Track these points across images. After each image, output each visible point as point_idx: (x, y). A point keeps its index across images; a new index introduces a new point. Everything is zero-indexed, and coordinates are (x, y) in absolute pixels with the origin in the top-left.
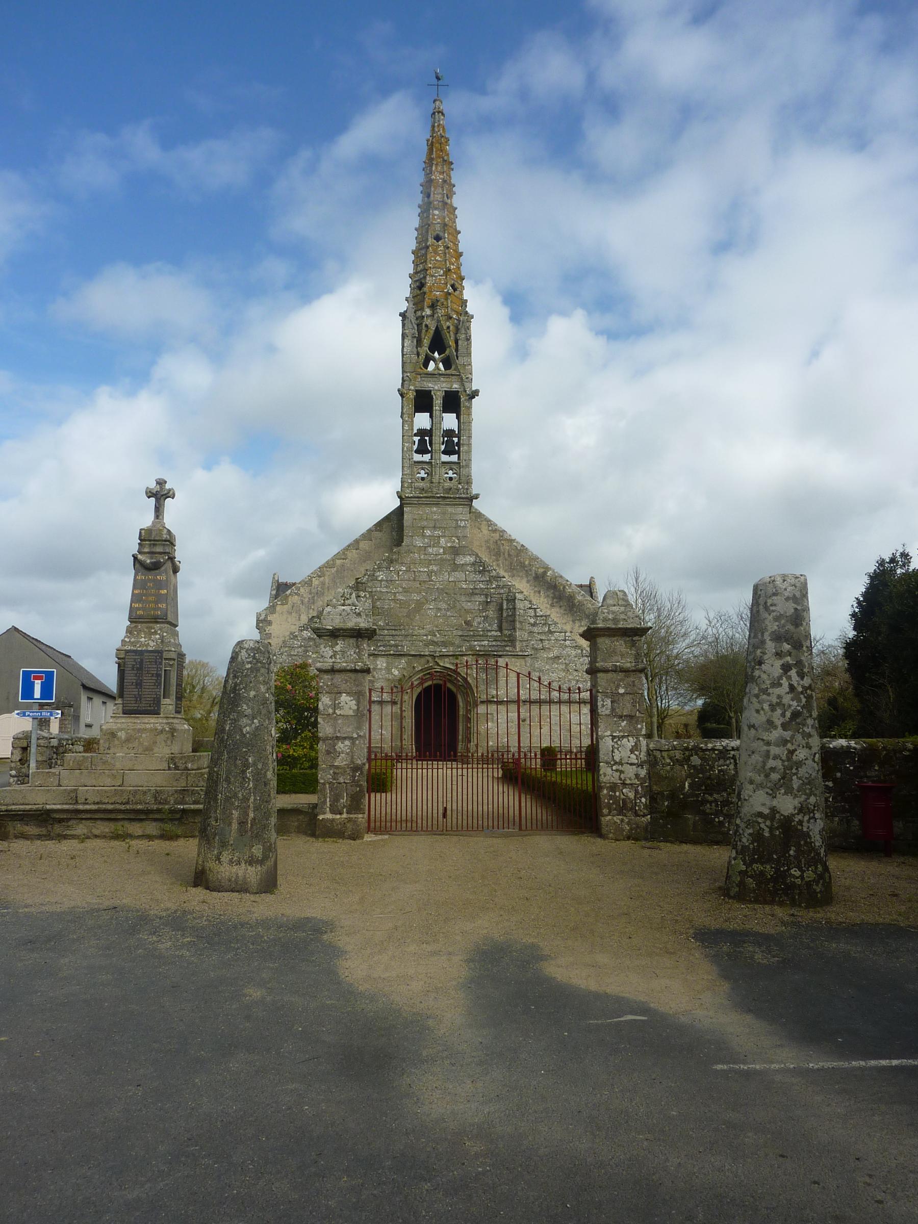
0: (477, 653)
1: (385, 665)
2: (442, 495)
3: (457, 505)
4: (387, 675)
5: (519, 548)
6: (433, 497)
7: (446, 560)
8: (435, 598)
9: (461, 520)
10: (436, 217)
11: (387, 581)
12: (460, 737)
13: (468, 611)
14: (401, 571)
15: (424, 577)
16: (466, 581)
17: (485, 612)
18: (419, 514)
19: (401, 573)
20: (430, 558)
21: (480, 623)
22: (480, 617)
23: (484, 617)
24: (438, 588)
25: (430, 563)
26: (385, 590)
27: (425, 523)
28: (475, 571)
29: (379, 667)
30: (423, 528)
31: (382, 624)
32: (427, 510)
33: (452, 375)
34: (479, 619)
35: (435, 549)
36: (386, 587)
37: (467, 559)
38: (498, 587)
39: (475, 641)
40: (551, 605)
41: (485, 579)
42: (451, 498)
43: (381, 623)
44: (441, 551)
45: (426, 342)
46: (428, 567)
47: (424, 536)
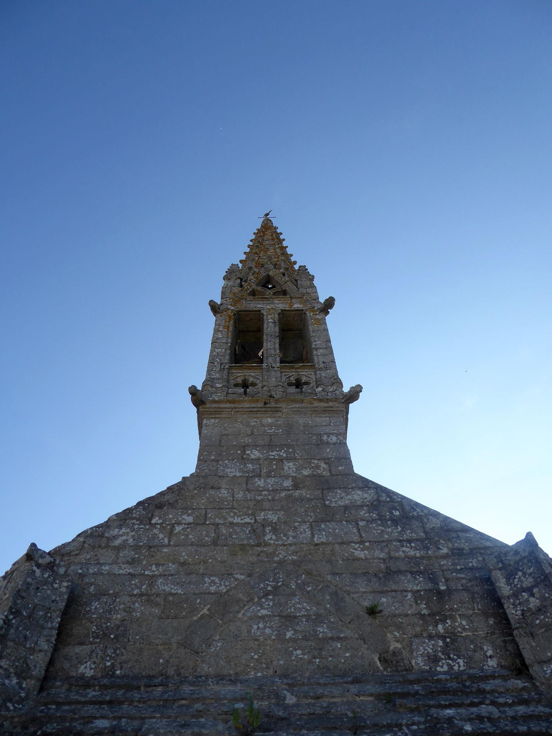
7: (301, 499)
8: (276, 588)
9: (328, 435)
14: (179, 523)
16: (362, 542)
17: (443, 621)
19: (178, 529)
20: (259, 498)
22: (430, 637)
23: (443, 638)
24: (281, 563)
26: (128, 569)
28: (381, 518)
30: (244, 448)
31: (89, 673)
34: (428, 647)
35: (271, 481)
36: (132, 562)
37: (356, 497)
44: (288, 483)
46: (253, 514)
47: (243, 459)
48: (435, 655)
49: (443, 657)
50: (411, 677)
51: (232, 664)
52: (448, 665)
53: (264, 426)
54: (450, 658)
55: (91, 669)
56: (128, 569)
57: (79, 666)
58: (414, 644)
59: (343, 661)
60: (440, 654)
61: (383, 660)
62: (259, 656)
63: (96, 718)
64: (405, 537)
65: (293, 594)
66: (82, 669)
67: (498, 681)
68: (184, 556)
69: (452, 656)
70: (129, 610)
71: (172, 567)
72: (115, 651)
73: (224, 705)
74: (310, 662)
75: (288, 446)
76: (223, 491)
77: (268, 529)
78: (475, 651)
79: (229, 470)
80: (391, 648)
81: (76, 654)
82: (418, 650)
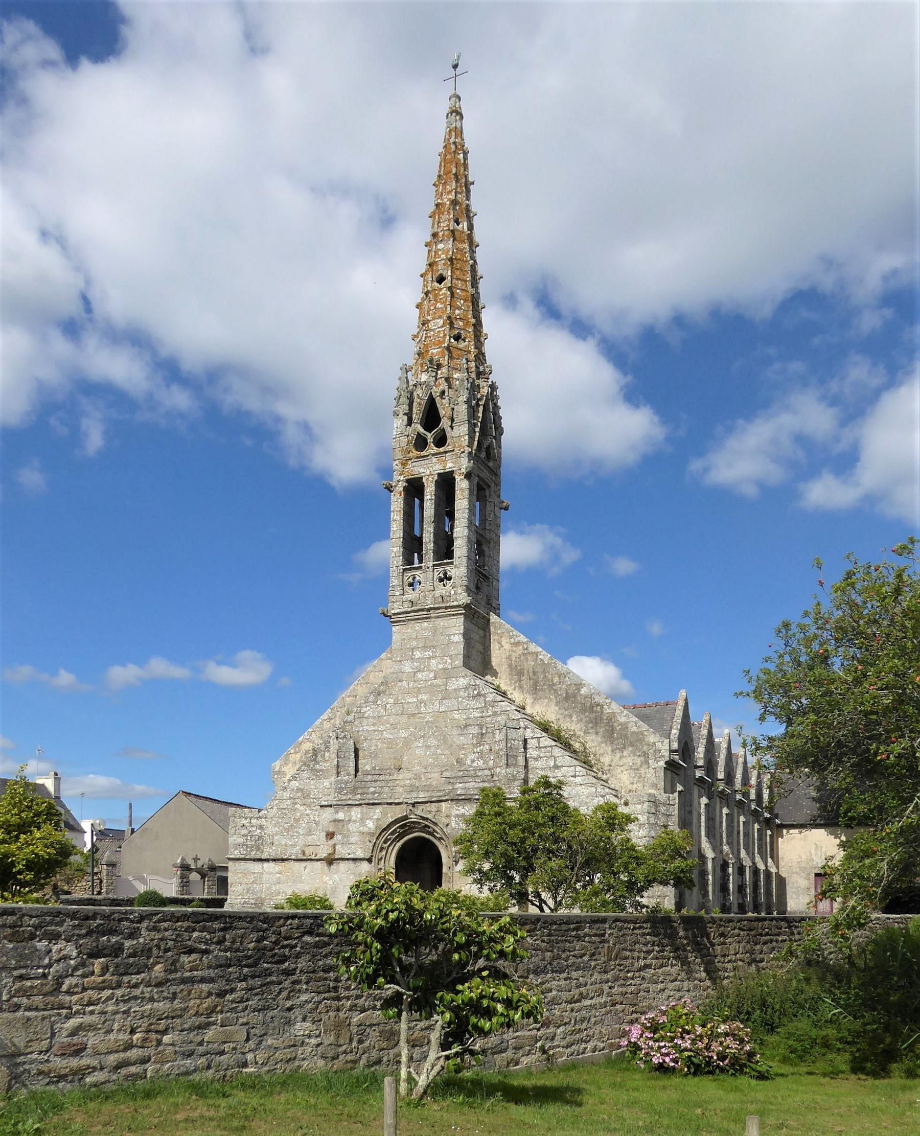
1: (359, 816)
2: (432, 606)
3: (450, 615)
5: (546, 662)
6: (422, 610)
9: (454, 635)
10: (440, 253)
11: (374, 718)
13: (461, 747)
15: (412, 709)
16: (458, 710)
18: (408, 633)
19: (388, 706)
25: (419, 691)
26: (372, 728)
27: (414, 643)
29: (354, 818)
32: (417, 626)
33: (446, 452)
36: (374, 724)
38: (495, 714)
39: (460, 783)
40: (585, 733)
41: (480, 706)
42: (441, 608)
43: (368, 768)
44: (432, 675)
45: (416, 416)
53: (422, 630)
56: (372, 728)
61: (457, 762)
64: (476, 707)
65: (430, 737)
66: (366, 767)
68: (392, 721)
70: (377, 746)
71: (388, 726)
75: (434, 647)
76: (404, 682)
77: (422, 704)
79: (406, 668)
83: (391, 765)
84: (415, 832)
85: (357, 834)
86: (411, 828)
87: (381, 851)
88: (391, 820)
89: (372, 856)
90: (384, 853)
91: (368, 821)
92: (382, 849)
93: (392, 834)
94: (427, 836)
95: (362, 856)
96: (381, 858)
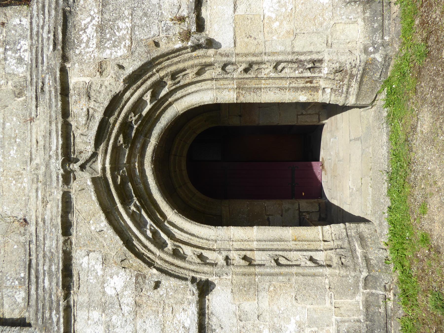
0: (59, 47)
1: (96, 314)
4: (126, 309)
12: (303, 98)
21: (20, 60)
34: (12, 61)
43: (20, 296)
48: (18, 59)
49: (19, 54)
50: (29, 78)
51: (18, 198)
52: (24, 51)
54: (20, 50)
55: (20, 294)
57: (17, 302)
58: (9, 72)
59: (18, 123)
60: (17, 55)
61: (20, 94)
62: (14, 180)
63: (44, 286)
66: (20, 300)
67: (34, 21)
69: (18, 48)
72: (9, 280)
73: (39, 203)
74: (19, 145)
78: (16, 31)
80: (11, 88)
81: (9, 307)
82: (13, 70)
83: (18, 242)
84: (143, 171)
85: (139, 322)
86: (131, 176)
87: (183, 257)
88: (104, 223)
89: (193, 280)
90: (187, 250)
91: (110, 291)
92: (176, 253)
93: (141, 225)
94: (153, 142)
95: (193, 309)
96: (200, 256)
